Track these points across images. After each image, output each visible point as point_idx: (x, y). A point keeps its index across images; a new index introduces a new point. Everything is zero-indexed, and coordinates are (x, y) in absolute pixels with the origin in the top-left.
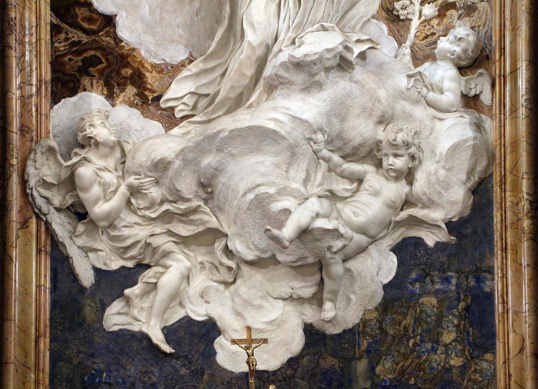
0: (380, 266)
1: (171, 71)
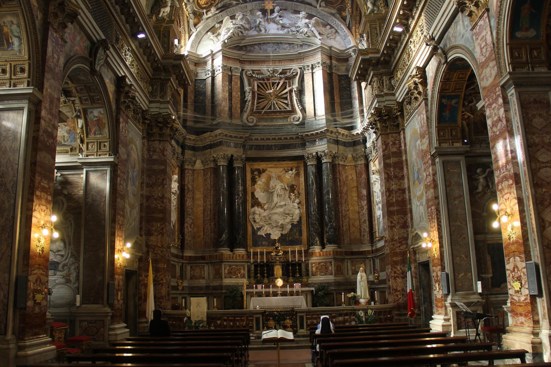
0: (290, 226)
1: (265, 204)
